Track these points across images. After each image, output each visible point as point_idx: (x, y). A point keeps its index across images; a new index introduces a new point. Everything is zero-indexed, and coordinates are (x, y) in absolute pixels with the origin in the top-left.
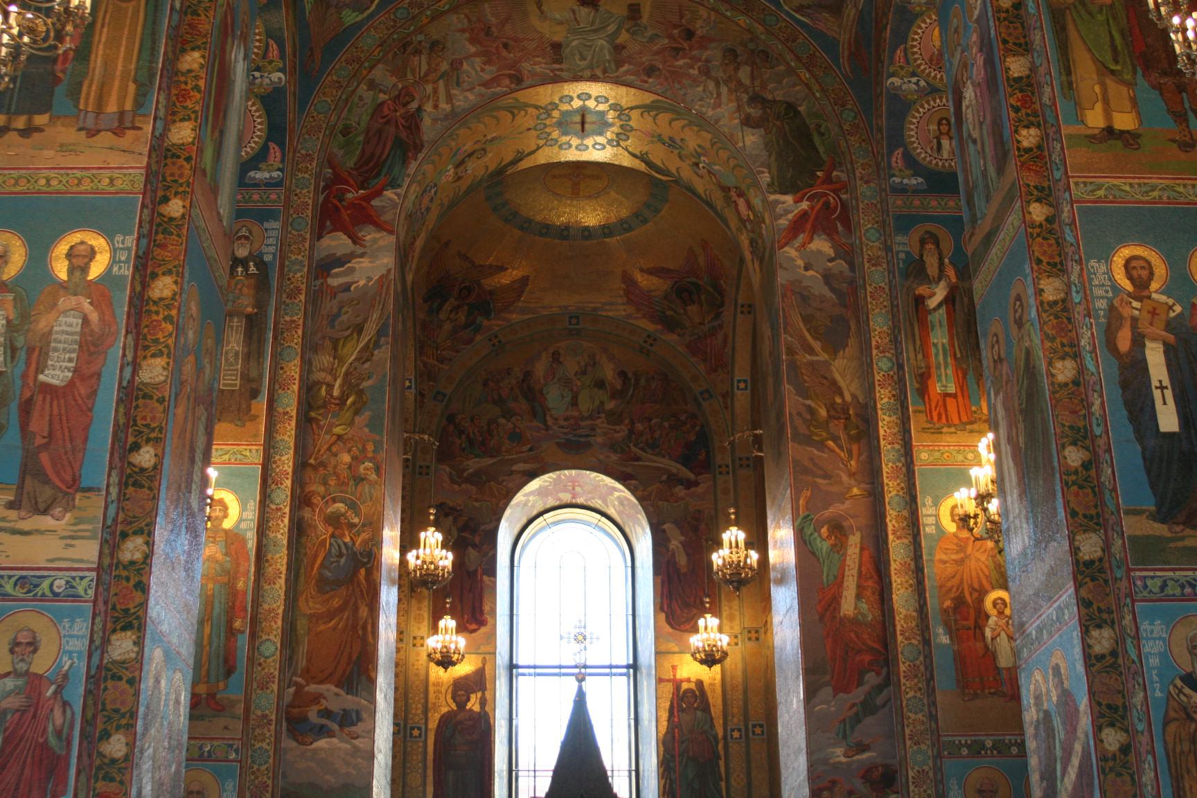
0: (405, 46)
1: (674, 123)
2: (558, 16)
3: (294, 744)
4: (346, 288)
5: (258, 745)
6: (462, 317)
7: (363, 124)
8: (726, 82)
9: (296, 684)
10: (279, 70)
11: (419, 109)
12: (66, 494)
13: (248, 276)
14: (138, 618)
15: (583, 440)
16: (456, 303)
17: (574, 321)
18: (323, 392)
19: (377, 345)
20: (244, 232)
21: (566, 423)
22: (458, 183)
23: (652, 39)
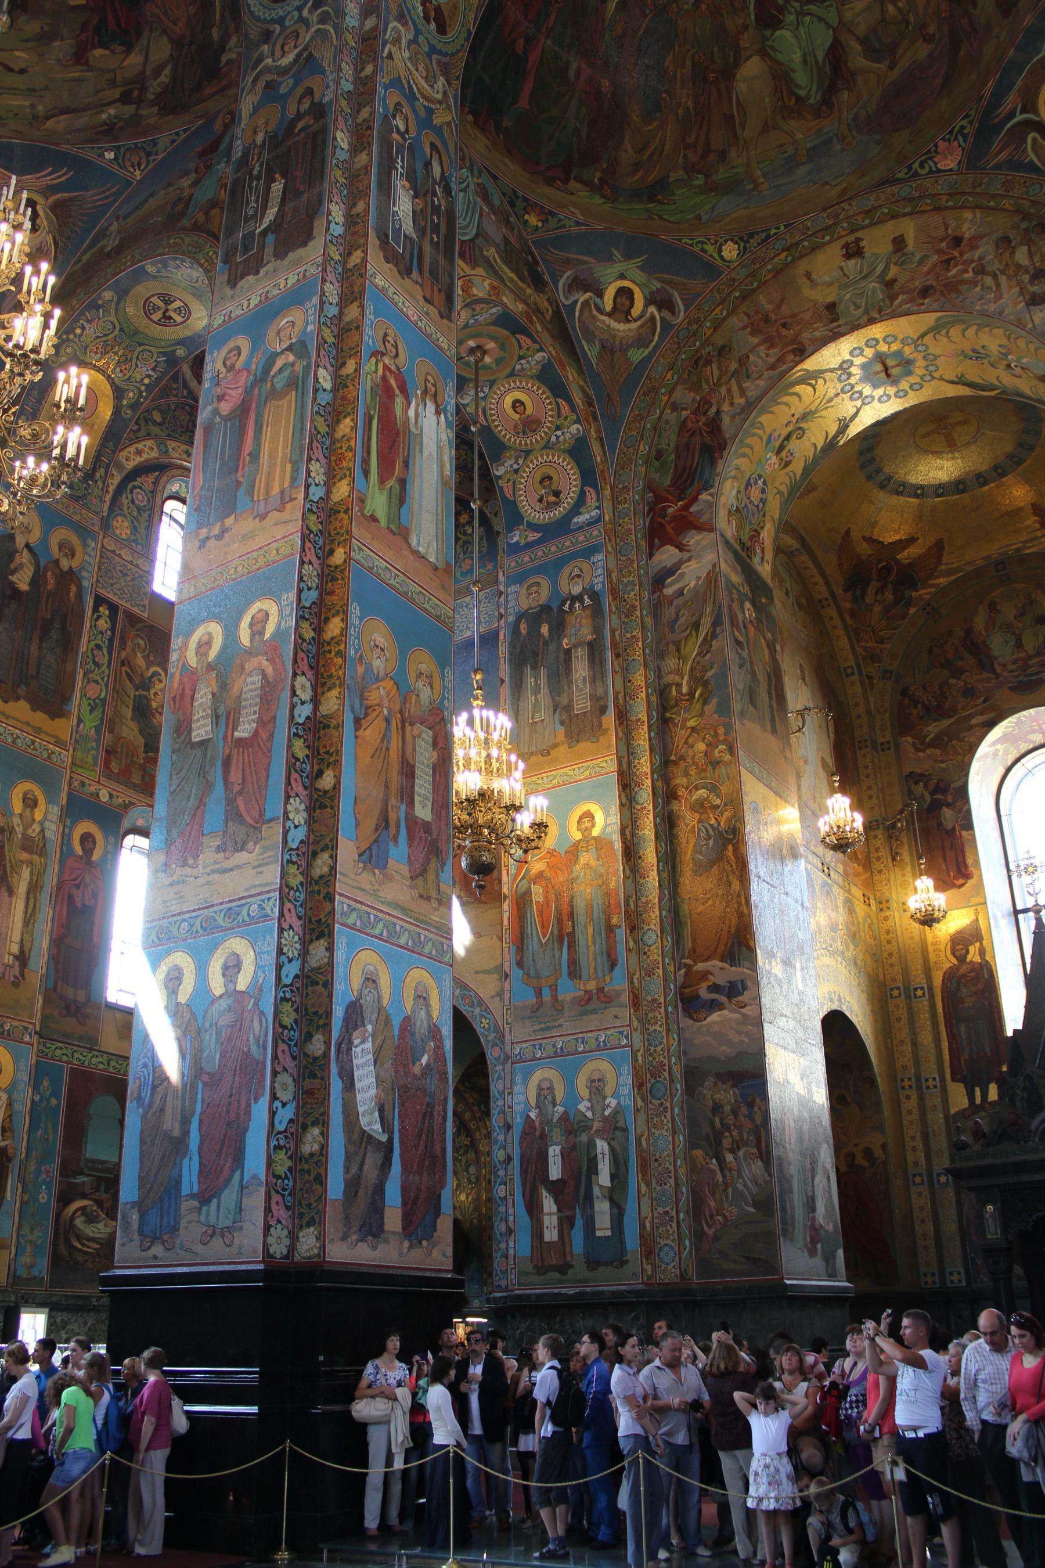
0: (696, 363)
1: (967, 333)
2: (827, 279)
3: (691, 1022)
4: (680, 593)
5: (652, 1029)
6: (889, 596)
7: (672, 445)
8: (1003, 272)
9: (686, 965)
10: (575, 422)
11: (718, 412)
12: (255, 828)
13: (584, 608)
14: (328, 926)
15: (1034, 678)
16: (879, 585)
17: (1000, 567)
18: (674, 693)
19: (714, 636)
20: (576, 572)
21: (1014, 667)
22: (790, 468)
23: (920, 263)
